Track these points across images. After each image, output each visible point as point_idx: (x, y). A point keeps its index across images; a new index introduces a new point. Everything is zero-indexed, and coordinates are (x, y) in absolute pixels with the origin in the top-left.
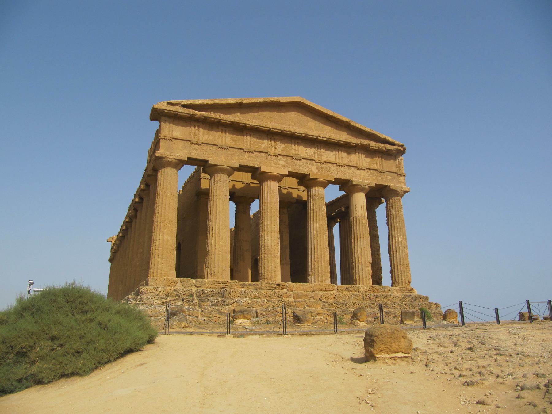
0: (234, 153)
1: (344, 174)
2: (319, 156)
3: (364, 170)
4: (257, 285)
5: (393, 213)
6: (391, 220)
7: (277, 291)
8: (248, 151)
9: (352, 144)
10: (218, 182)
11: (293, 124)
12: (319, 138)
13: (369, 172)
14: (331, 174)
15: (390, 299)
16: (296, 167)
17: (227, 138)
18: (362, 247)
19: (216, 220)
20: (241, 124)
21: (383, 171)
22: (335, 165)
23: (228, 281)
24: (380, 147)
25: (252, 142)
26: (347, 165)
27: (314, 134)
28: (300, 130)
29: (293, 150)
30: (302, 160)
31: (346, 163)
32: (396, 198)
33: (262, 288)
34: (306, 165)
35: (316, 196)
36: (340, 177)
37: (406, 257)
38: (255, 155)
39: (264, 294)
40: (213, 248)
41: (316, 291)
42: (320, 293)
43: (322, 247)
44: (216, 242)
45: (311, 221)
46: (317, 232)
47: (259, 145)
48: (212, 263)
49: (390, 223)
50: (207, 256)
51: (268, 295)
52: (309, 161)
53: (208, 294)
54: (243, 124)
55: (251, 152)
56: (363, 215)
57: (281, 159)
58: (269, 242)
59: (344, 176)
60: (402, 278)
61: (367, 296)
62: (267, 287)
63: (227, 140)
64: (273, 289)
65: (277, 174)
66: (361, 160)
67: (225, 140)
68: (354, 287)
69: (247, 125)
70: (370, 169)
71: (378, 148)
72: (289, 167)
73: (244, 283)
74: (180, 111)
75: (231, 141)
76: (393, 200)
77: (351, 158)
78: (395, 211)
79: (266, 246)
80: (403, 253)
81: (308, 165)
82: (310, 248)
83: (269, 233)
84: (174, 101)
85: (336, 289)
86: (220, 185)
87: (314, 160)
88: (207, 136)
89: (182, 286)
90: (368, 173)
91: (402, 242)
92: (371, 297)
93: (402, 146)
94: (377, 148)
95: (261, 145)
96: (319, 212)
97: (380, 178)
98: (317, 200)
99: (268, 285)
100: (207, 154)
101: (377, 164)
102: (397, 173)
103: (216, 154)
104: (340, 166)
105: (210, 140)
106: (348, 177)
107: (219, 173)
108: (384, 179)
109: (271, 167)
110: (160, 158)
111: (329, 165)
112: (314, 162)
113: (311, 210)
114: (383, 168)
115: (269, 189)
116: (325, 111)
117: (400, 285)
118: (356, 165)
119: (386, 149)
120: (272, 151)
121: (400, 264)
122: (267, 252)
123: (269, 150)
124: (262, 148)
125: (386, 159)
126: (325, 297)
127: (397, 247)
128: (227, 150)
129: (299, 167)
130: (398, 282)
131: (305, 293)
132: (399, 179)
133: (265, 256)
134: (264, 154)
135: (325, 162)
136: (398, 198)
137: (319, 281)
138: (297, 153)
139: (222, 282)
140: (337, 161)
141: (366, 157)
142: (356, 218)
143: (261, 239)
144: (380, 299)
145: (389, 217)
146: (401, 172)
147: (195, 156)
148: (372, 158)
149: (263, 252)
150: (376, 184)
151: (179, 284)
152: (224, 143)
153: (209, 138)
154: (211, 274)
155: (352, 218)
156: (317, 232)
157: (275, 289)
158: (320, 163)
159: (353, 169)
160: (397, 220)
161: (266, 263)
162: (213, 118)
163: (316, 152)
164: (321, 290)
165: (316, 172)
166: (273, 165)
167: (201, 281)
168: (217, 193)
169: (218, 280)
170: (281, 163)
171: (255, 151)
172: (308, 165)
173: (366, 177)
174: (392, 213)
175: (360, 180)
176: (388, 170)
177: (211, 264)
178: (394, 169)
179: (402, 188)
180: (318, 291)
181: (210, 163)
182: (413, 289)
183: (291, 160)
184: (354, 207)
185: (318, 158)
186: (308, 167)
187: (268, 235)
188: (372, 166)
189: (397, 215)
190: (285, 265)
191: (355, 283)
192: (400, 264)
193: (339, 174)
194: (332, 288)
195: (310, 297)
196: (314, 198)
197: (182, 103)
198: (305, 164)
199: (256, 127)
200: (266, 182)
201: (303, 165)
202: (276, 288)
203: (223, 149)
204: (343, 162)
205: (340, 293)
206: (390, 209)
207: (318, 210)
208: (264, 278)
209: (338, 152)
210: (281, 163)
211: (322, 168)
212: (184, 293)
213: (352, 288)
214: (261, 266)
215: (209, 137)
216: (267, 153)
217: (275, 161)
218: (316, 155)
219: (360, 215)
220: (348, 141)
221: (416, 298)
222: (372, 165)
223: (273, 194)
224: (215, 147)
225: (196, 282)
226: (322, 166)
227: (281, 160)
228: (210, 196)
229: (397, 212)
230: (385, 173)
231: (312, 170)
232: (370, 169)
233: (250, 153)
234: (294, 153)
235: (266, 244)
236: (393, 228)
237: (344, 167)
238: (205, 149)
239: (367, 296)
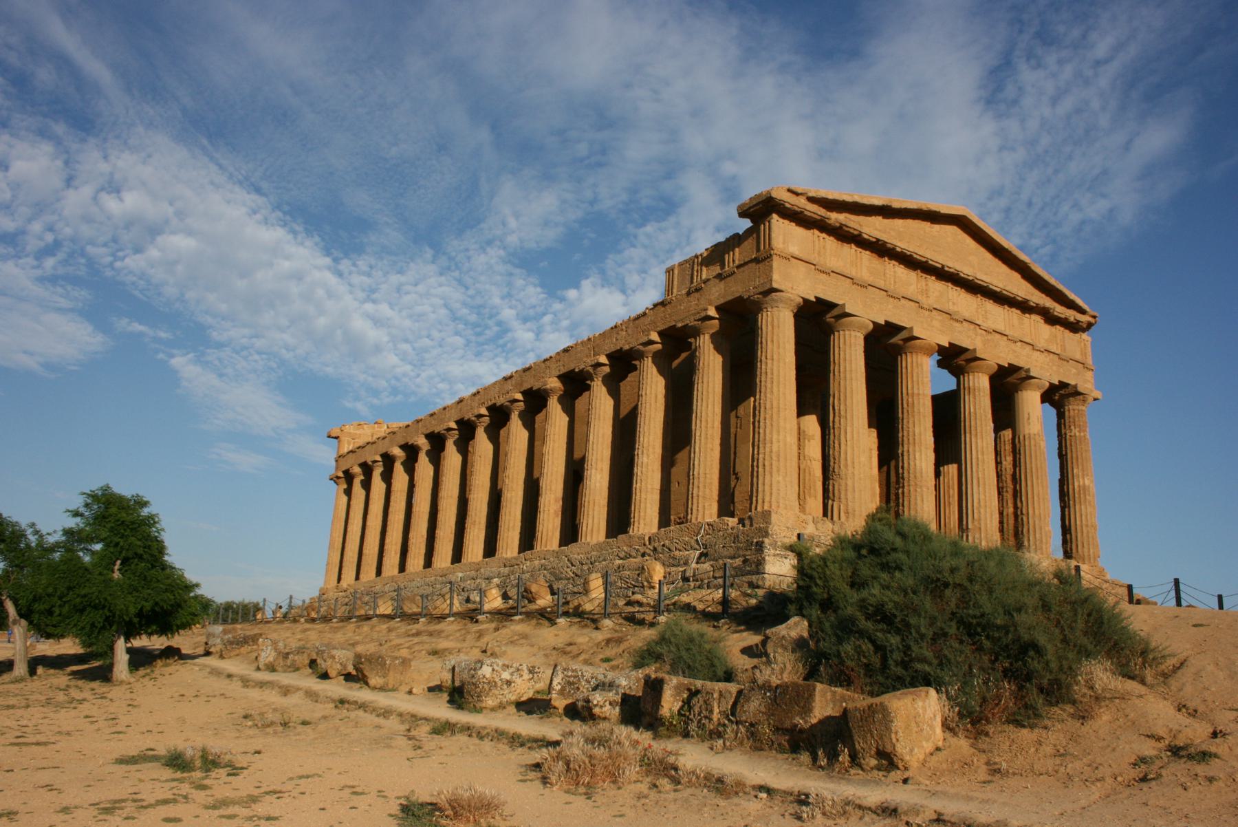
58: (924, 465)
79: (918, 470)
98: (982, 399)
149: (912, 483)
161: (919, 502)
196: (977, 393)
207: (983, 417)
235: (918, 468)
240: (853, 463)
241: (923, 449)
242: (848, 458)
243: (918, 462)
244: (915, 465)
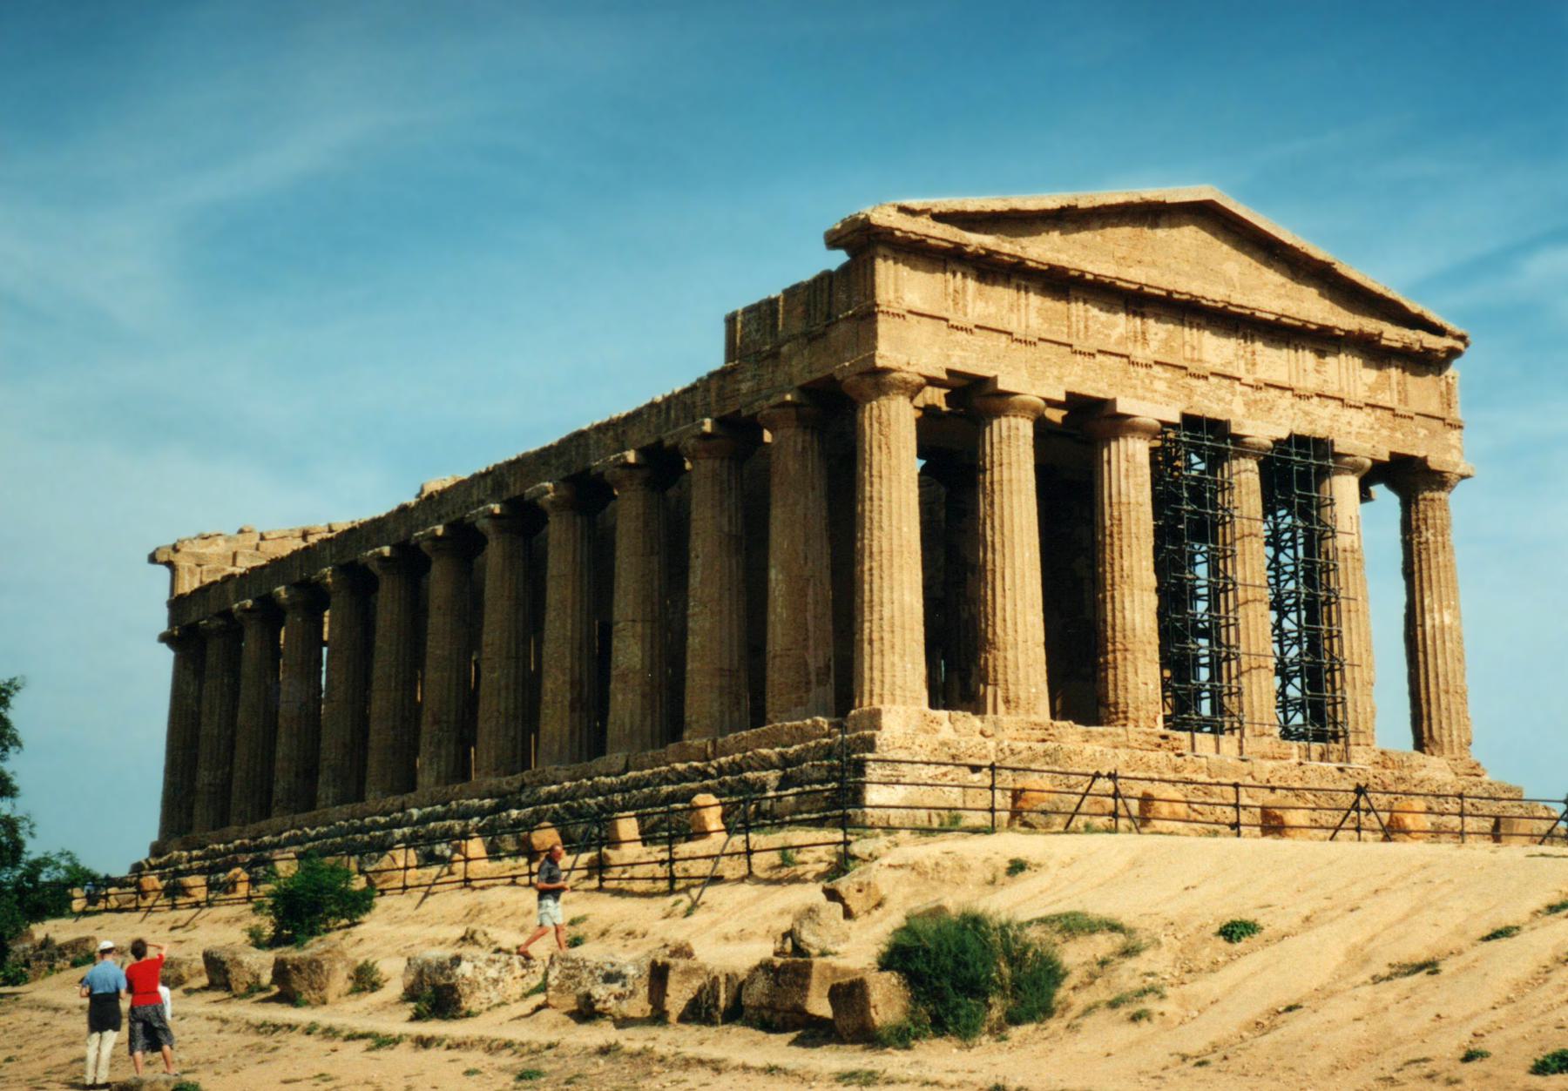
4: (1119, 735)
6: (1420, 561)
8: (1083, 350)
9: (1338, 332)
10: (1013, 441)
11: (1188, 268)
12: (1258, 314)
18: (1355, 637)
19: (1013, 554)
20: (1072, 273)
22: (1289, 393)
27: (1245, 303)
28: (1213, 292)
29: (1187, 348)
30: (1212, 379)
40: (1010, 631)
42: (1270, 764)
49: (1416, 567)
51: (1152, 763)
52: (1226, 382)
53: (1021, 756)
54: (1077, 274)
56: (1356, 546)
67: (1026, 314)
69: (1089, 277)
70: (1374, 406)
74: (933, 232)
75: (1040, 321)
79: (1128, 627)
81: (1222, 393)
84: (915, 203)
87: (1239, 379)
89: (951, 731)
93: (1462, 338)
94: (1398, 345)
97: (1399, 435)
99: (1143, 737)
102: (1443, 419)
105: (989, 315)
106: (1320, 432)
107: (1015, 416)
109: (1137, 397)
110: (886, 371)
111: (1274, 392)
112: (1237, 383)
116: (1273, 232)
117: (1446, 751)
118: (1337, 395)
119: (1422, 347)
121: (1447, 692)
123: (1129, 349)
124: (1112, 340)
125: (1414, 374)
126: (1279, 774)
132: (1449, 436)
134: (1118, 359)
141: (1365, 366)
143: (1109, 606)
148: (1379, 368)
150: (1393, 455)
151: (947, 724)
158: (1252, 386)
159: (1333, 404)
161: (1130, 676)
162: (1009, 255)
166: (1140, 392)
170: (1161, 386)
171: (1100, 351)
172: (1222, 393)
174: (1423, 540)
176: (1422, 410)
177: (1005, 673)
178: (1434, 407)
179: (1457, 465)
182: (1478, 765)
185: (1248, 371)
186: (1221, 400)
193: (1297, 422)
197: (936, 210)
199: (1107, 280)
200: (1122, 441)
202: (1159, 746)
206: (1418, 527)
209: (1296, 351)
212: (970, 752)
216: (1128, 357)
220: (1329, 323)
224: (1004, 337)
226: (1259, 395)
227: (1160, 379)
229: (1440, 539)
230: (1412, 418)
232: (1374, 406)
236: (1425, 585)
240: (1016, 624)
241: (1136, 592)
242: (1008, 618)
243: (1128, 613)
244: (1124, 618)
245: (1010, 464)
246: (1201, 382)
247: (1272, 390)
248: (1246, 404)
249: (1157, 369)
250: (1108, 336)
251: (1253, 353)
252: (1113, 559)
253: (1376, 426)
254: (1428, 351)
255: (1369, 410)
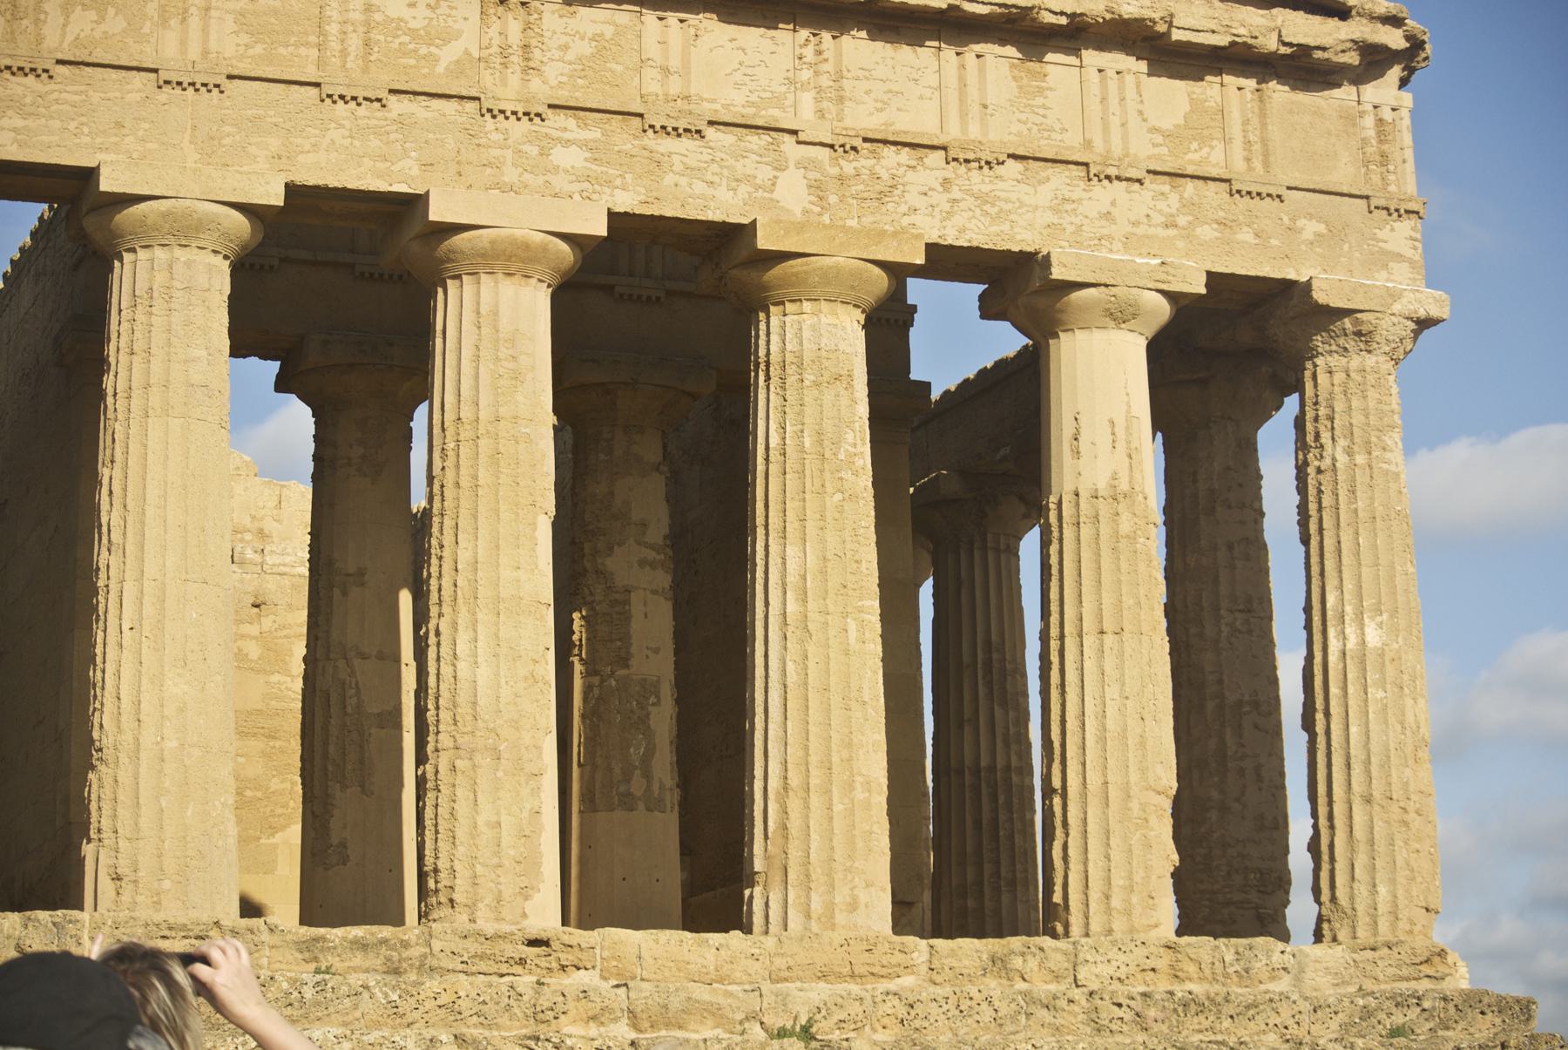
0: (261, 112)
1: (996, 218)
2: (825, 104)
3: (1140, 181)
4: (406, 945)
5: (1334, 459)
6: (1320, 509)
7: (525, 981)
9: (1048, 18)
10: (158, 302)
13: (1174, 198)
14: (905, 221)
15: (1278, 1021)
16: (669, 179)
17: (213, 21)
18: (1112, 692)
21: (1264, 190)
23: (216, 923)
24: (1242, 31)
25: (375, 35)
26: (1010, 156)
29: (650, 73)
30: (710, 132)
31: (1012, 138)
32: (1355, 361)
33: (435, 963)
34: (739, 166)
35: (800, 365)
36: (969, 235)
37: (1409, 749)
38: (393, 115)
39: (440, 1002)
41: (786, 980)
43: (836, 700)
44: (145, 680)
45: (767, 534)
46: (804, 599)
47: (423, 50)
48: (120, 811)
50: (93, 768)
51: (464, 1004)
52: (756, 141)
55: (365, 99)
56: (1124, 486)
57: (567, 135)
58: (484, 674)
59: (994, 229)
60: (1374, 886)
61: (1120, 1005)
62: (465, 959)
63: (213, 36)
64: (504, 968)
65: (540, 237)
66: (1115, 121)
67: (205, 30)
68: (1042, 949)
71: (1230, 39)
72: (618, 182)
73: (322, 931)
75: (245, 38)
76: (1339, 377)
77: (1044, 107)
78: (1349, 452)
79: (463, 698)
80: (1386, 722)
81: (747, 166)
82: (759, 709)
83: (480, 616)
85: (924, 968)
86: (170, 323)
87: (794, 132)
88: (92, 15)
90: (1161, 205)
91: (1382, 655)
92: (1152, 1013)
94: (1221, 40)
95: (433, 49)
96: (822, 471)
99: (473, 946)
100: (86, 130)
101: (1227, 141)
103: (146, 126)
104: (967, 161)
108: (1274, 242)
113: (772, 458)
114: (1266, 164)
115: (484, 330)
120: (507, 90)
121: (1368, 800)
122: (467, 738)
124: (440, 69)
127: (1351, 690)
128: (216, 91)
129: (683, 181)
130: (1349, 911)
131: (702, 993)
132: (1380, 234)
133: (459, 763)
134: (453, 105)
135: (865, 140)
136: (1370, 360)
137: (808, 916)
138: (675, 86)
139: (184, 927)
140: (952, 133)
142: (1078, 505)
144: (1206, 1024)
145: (1312, 491)
146: (1392, 188)
147: (14, 148)
152: (194, 52)
153: (103, 27)
154: (117, 878)
155: (1053, 499)
156: (804, 599)
157: (518, 969)
158: (832, 146)
159: (1059, 179)
160: (1356, 510)
161: (462, 808)
163: (806, 74)
164: (823, 976)
165: (806, 212)
166: (510, 175)
167: (54, 924)
168: (148, 373)
169: (158, 918)
170: (569, 158)
172: (747, 166)
173: (1152, 231)
174: (1326, 463)
175: (1104, 254)
178: (1344, 174)
179: (1395, 296)
180: (800, 979)
181: (103, 188)
183: (636, 137)
184: (1068, 430)
185: (821, 113)
186: (749, 179)
187: (475, 631)
188: (1190, 156)
189: (1361, 478)
190: (641, 806)
191: (1060, 928)
192: (1368, 800)
193: (958, 220)
194: (894, 961)
195: (740, 1016)
198: (731, 161)
201: (715, 167)
202: (522, 962)
203: (191, 89)
204: (992, 136)
205: (947, 990)
206: (1317, 436)
207: (811, 465)
208: (451, 901)
210: (569, 158)
211: (841, 179)
213: (1029, 957)
214: (436, 825)
215: (102, 19)
217: (526, 148)
218: (807, 100)
219: (1103, 487)
221: (1452, 1010)
222: (1195, 145)
223: (511, 365)
225: (26, 926)
226: (848, 166)
227: (567, 143)
228: (110, 391)
229: (1360, 459)
231: (775, 196)
233: (359, 105)
234: (652, 86)
235: (463, 685)
236: (1330, 564)
237: (999, 170)
238: (77, 98)
239: (1120, 1005)
245: (148, 351)
246: (686, 143)
247: (889, 151)
248: (817, 188)
249: (557, 120)
250: (433, 60)
251: (839, 77)
252: (442, 547)
253: (1182, 220)
254: (1304, 50)
255: (1164, 185)
